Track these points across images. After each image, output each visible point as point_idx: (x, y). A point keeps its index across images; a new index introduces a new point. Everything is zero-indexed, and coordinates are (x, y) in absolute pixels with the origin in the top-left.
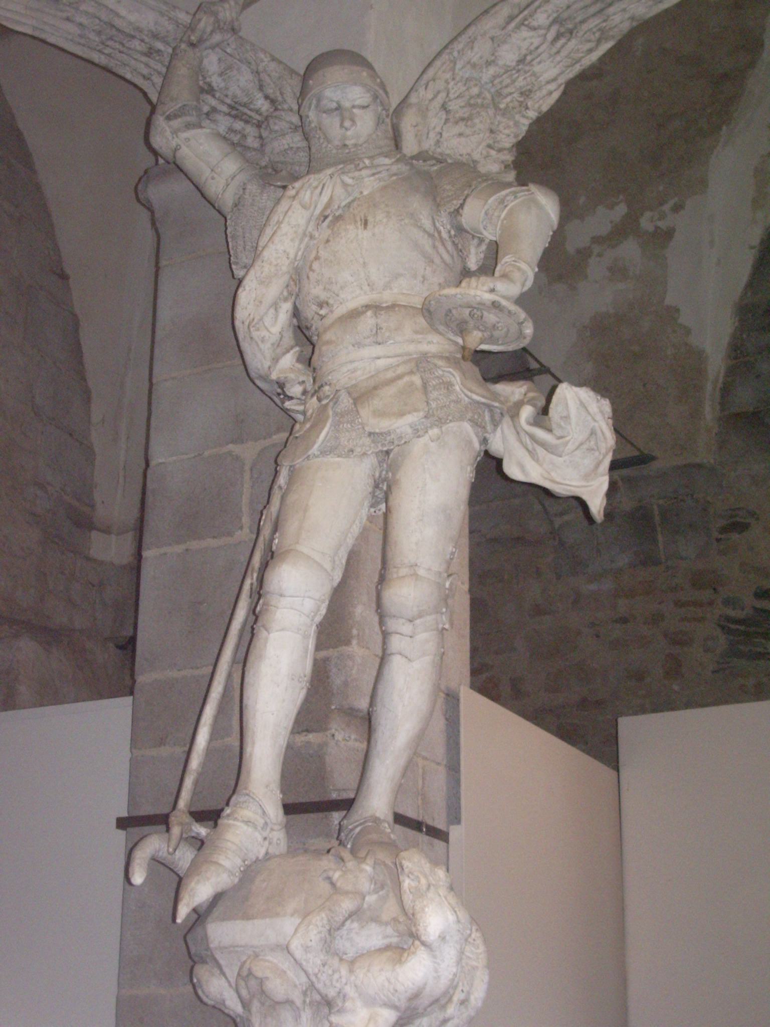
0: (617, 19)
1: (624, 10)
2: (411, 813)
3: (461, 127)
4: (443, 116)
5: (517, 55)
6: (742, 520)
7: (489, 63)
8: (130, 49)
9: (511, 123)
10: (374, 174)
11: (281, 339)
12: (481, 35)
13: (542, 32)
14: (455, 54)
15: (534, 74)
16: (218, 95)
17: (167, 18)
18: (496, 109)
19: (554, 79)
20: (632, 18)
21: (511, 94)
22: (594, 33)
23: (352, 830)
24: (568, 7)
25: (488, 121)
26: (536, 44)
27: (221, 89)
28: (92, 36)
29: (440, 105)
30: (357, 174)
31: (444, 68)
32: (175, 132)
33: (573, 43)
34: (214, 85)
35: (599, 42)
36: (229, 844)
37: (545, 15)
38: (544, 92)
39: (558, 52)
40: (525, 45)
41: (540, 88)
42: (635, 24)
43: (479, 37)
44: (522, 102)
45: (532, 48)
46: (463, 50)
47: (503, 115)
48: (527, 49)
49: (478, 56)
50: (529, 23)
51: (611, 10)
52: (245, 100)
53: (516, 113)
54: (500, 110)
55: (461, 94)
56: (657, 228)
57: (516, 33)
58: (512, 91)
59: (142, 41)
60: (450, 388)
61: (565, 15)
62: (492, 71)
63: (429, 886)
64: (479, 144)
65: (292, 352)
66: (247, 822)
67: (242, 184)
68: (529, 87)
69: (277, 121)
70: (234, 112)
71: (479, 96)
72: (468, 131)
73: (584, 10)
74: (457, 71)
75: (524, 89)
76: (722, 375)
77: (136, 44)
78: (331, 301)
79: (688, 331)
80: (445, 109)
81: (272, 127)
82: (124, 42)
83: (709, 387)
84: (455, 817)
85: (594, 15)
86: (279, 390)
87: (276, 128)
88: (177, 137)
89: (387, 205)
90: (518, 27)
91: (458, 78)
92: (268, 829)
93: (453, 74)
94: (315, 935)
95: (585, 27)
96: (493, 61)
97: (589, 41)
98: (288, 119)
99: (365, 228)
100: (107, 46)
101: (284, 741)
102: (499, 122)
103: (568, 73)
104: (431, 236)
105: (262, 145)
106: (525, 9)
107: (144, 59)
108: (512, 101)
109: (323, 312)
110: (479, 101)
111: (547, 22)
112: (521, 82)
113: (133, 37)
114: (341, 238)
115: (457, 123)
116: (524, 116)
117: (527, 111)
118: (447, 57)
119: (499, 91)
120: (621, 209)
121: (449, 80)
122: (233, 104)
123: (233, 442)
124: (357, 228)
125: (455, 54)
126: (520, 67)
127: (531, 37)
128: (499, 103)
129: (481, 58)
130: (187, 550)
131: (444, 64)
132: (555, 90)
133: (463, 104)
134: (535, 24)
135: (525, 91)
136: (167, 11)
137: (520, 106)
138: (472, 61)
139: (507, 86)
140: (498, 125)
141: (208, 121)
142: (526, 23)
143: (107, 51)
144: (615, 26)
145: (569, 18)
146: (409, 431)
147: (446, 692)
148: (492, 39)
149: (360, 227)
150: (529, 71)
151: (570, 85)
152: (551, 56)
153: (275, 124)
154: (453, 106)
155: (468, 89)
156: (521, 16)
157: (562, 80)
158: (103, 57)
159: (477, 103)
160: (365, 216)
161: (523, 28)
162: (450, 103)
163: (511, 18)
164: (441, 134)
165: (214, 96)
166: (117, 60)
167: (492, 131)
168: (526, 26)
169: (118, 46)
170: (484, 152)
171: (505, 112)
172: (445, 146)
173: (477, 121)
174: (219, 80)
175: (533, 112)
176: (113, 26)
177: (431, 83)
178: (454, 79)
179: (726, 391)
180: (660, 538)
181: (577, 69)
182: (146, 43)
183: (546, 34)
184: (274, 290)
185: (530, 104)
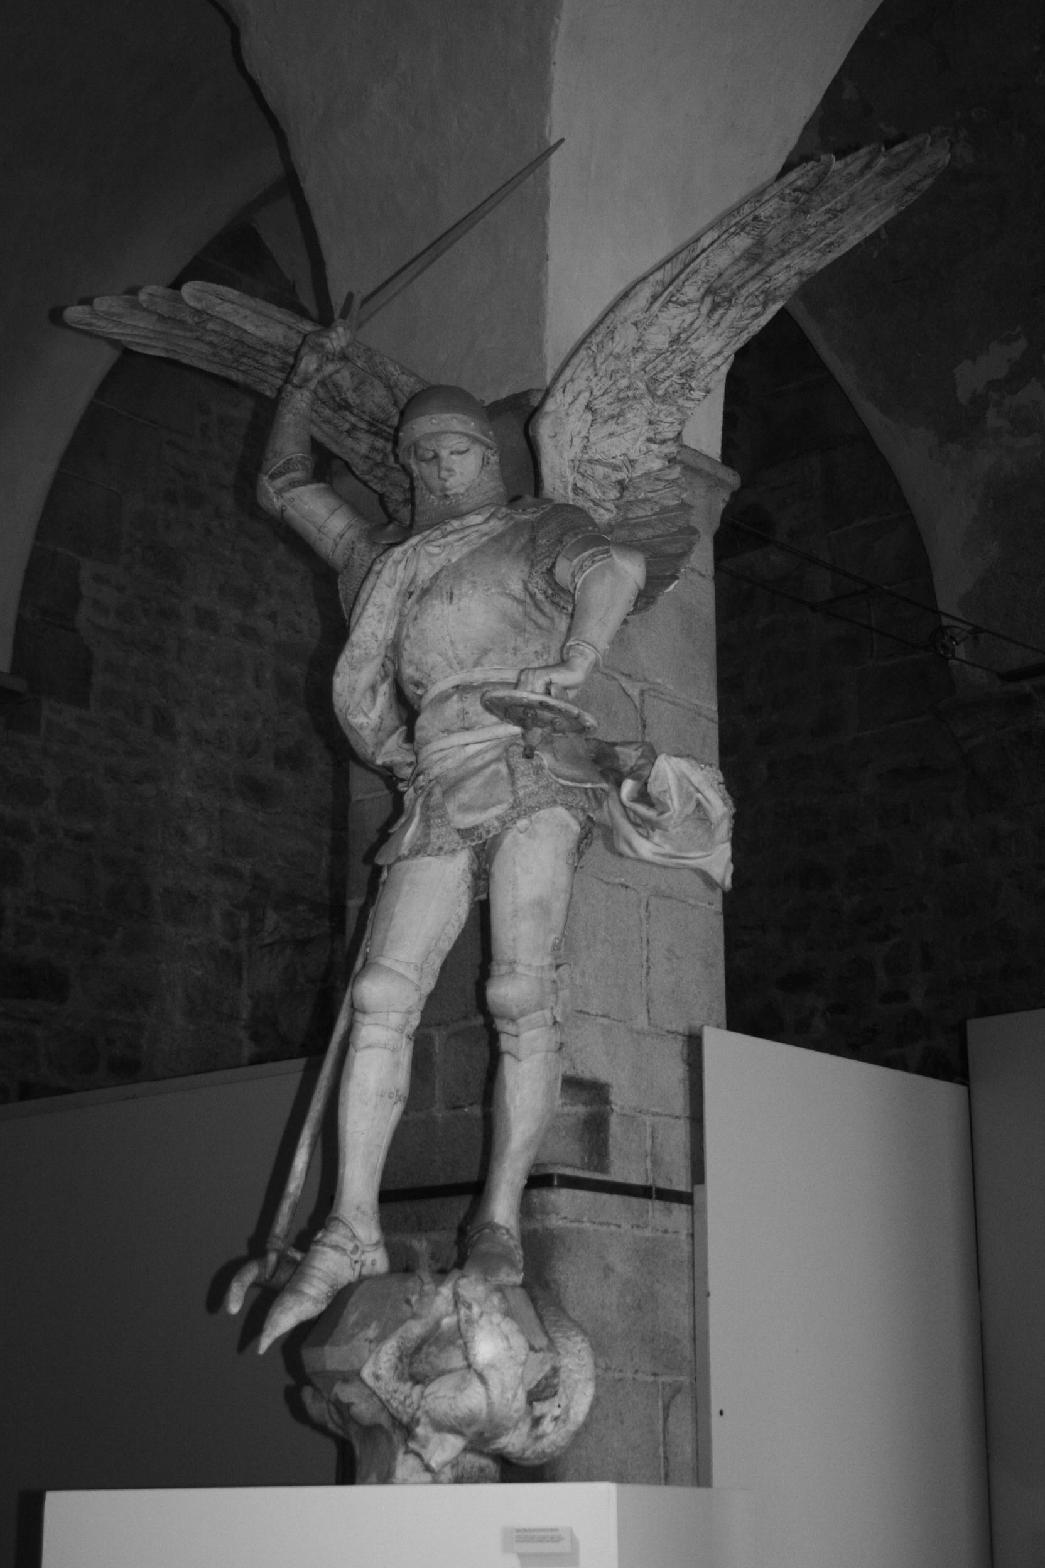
0: (782, 277)
3: (611, 426)
4: (589, 417)
5: (668, 336)
7: (635, 351)
8: (263, 365)
9: (674, 409)
10: (462, 539)
11: (381, 723)
12: (622, 323)
13: (696, 306)
14: (594, 348)
15: (693, 352)
16: (355, 411)
17: (295, 331)
18: (653, 397)
19: (720, 353)
20: (800, 273)
21: (668, 378)
22: (757, 297)
23: (473, 1236)
24: (720, 275)
25: (645, 413)
27: (358, 405)
28: (225, 354)
29: (583, 407)
30: (442, 541)
31: (583, 365)
32: (280, 492)
33: (733, 313)
34: (350, 401)
35: (765, 305)
38: (709, 368)
39: (718, 324)
40: (675, 324)
41: (703, 365)
42: (805, 279)
43: (619, 326)
44: (684, 384)
45: (685, 325)
46: (602, 342)
47: (663, 402)
48: (679, 328)
49: (621, 345)
50: (678, 299)
51: (772, 270)
52: (382, 416)
53: (679, 397)
55: (607, 389)
57: (663, 312)
58: (668, 375)
60: (540, 772)
62: (641, 357)
63: (481, 1315)
64: (636, 440)
65: (398, 732)
66: (336, 1247)
68: (689, 367)
70: (373, 430)
71: (628, 388)
72: (620, 429)
73: (740, 274)
74: (598, 365)
75: (683, 371)
77: (269, 360)
78: (424, 682)
84: (698, 1173)
85: (753, 278)
88: (282, 497)
90: (664, 306)
91: (601, 374)
92: (359, 1252)
93: (595, 370)
94: (385, 1363)
95: (744, 292)
96: (641, 348)
97: (754, 306)
99: (451, 603)
100: (241, 363)
101: (378, 1159)
102: (658, 410)
103: (735, 344)
104: (521, 602)
106: (670, 284)
108: (671, 385)
111: (699, 295)
112: (678, 363)
113: (266, 353)
114: (428, 615)
115: (606, 422)
116: (688, 399)
117: (692, 392)
118: (585, 353)
119: (654, 377)
121: (592, 377)
122: (371, 420)
124: (443, 603)
125: (594, 348)
126: (674, 347)
127: (682, 314)
128: (656, 390)
129: (625, 347)
132: (722, 364)
133: (611, 400)
134: (684, 299)
135: (686, 372)
136: (294, 323)
137: (683, 388)
138: (615, 352)
139: (662, 371)
140: (658, 415)
141: (350, 440)
142: (674, 299)
144: (781, 286)
145: (725, 285)
146: (496, 824)
147: (687, 1033)
148: (635, 324)
149: (445, 601)
150: (686, 350)
151: (740, 354)
152: (709, 329)
154: (599, 404)
156: (666, 293)
157: (729, 352)
159: (628, 396)
160: (451, 589)
162: (595, 402)
163: (655, 298)
164: (587, 438)
165: (352, 412)
166: (255, 377)
167: (651, 423)
168: (674, 302)
170: (644, 448)
171: (664, 399)
172: (594, 450)
173: (629, 416)
174: (354, 396)
176: (243, 343)
177: (568, 385)
178: (596, 375)
181: (745, 337)
183: (699, 308)
184: (368, 674)
185: (693, 384)
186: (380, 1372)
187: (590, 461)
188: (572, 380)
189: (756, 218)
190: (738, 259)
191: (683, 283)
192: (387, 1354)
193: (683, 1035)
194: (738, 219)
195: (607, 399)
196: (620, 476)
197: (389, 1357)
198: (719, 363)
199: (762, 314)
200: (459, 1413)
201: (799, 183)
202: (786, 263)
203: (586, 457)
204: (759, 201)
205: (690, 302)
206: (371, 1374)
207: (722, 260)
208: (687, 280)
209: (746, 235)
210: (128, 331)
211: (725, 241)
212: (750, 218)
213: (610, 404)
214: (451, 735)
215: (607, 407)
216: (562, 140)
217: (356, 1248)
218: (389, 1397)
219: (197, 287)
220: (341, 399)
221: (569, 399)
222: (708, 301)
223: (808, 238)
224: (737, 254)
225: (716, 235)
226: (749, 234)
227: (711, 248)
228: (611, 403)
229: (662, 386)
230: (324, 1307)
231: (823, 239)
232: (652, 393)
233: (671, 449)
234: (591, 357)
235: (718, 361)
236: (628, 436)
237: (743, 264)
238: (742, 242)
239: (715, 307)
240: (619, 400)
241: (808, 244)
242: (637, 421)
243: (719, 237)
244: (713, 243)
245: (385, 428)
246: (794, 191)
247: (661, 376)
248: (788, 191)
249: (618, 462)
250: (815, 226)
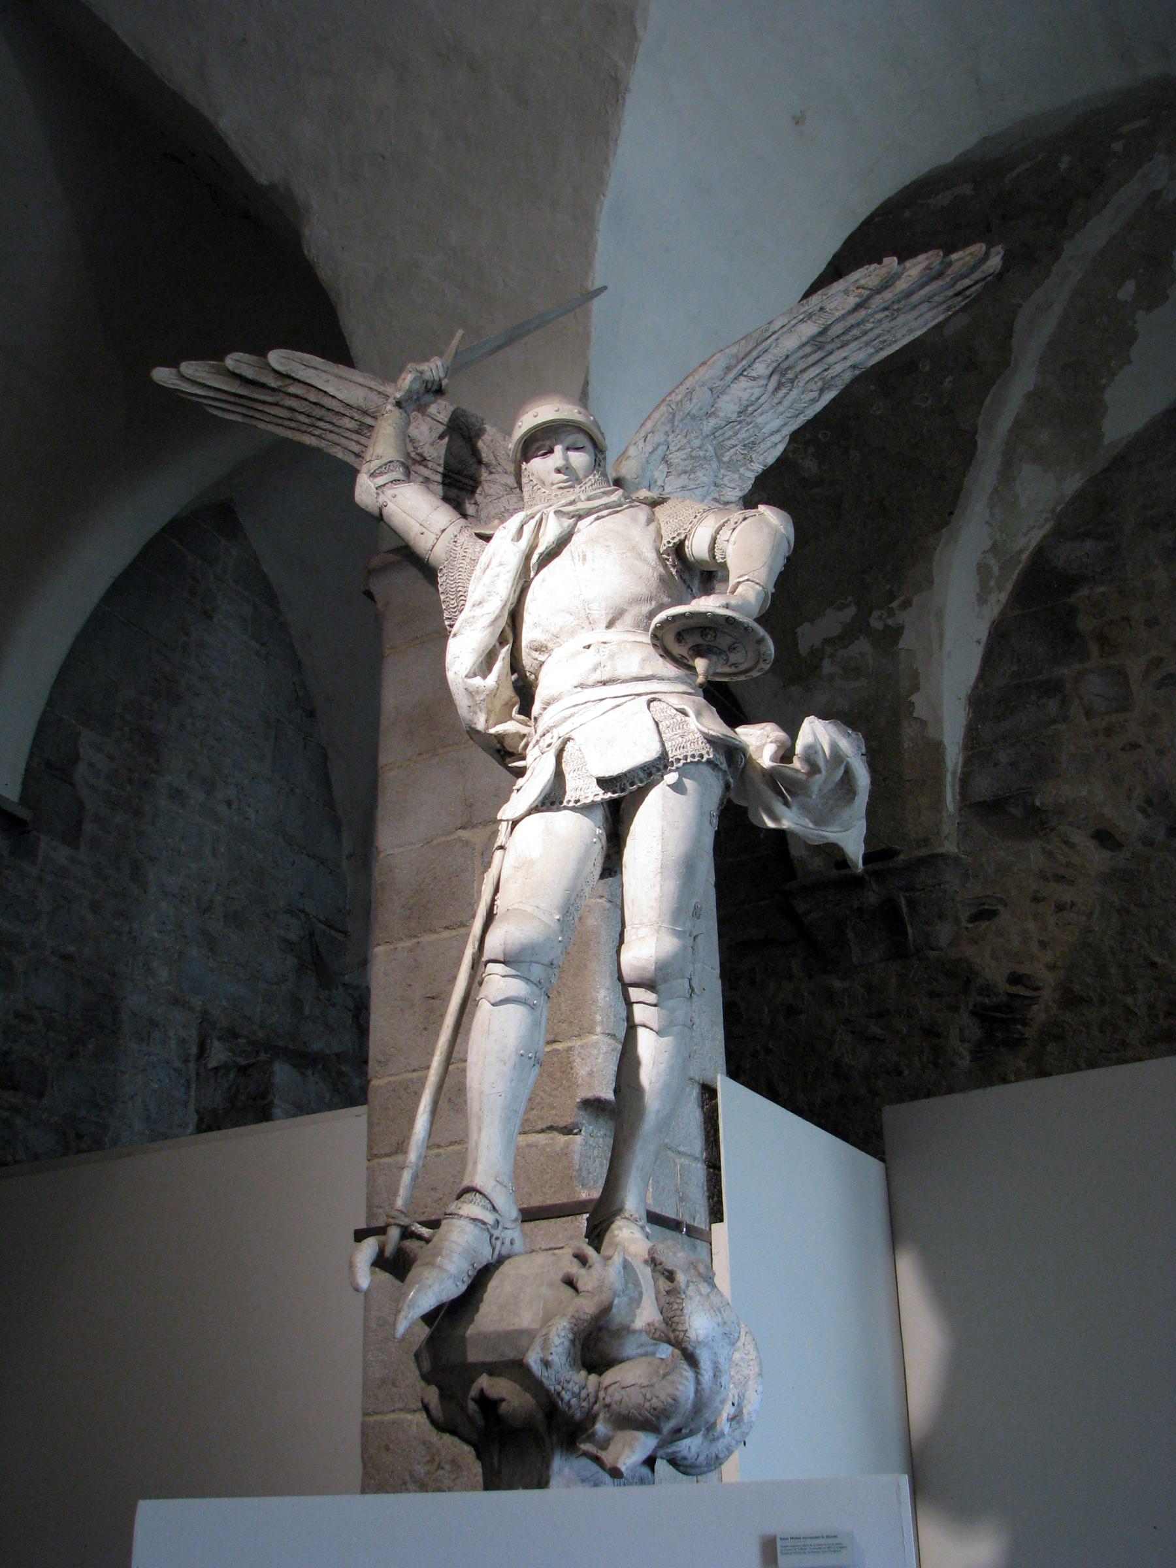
0: (838, 368)
1: (845, 358)
2: (669, 1212)
3: (683, 480)
5: (737, 406)
6: (991, 908)
7: (708, 415)
9: (736, 476)
13: (763, 382)
15: (756, 426)
16: (430, 464)
19: (778, 431)
20: (854, 367)
21: (734, 446)
24: (787, 357)
26: (756, 395)
34: (426, 455)
35: (822, 391)
36: (454, 1246)
37: (764, 366)
38: (768, 444)
39: (780, 403)
40: (745, 395)
42: (857, 372)
43: (697, 388)
45: (753, 399)
46: (681, 401)
48: (748, 400)
53: (741, 466)
54: (724, 463)
56: (886, 626)
59: (352, 418)
60: (685, 727)
61: (785, 365)
62: (713, 422)
67: (452, 537)
68: (752, 439)
69: (492, 485)
74: (676, 423)
76: (960, 765)
79: (923, 723)
80: (667, 462)
81: (486, 491)
82: (335, 421)
83: (949, 778)
84: (716, 1214)
85: (813, 365)
86: (498, 746)
87: (491, 491)
89: (606, 540)
91: (677, 432)
93: (673, 426)
96: (713, 413)
97: (812, 391)
98: (503, 481)
99: (583, 564)
105: (477, 511)
107: (355, 437)
109: (542, 658)
110: (702, 453)
111: (768, 372)
116: (748, 469)
120: (852, 610)
123: (463, 828)
125: (674, 406)
126: (742, 418)
127: (753, 387)
128: (722, 455)
129: (701, 409)
130: (418, 943)
133: (684, 457)
134: (754, 374)
138: (691, 413)
139: (729, 439)
142: (745, 373)
143: (317, 432)
145: (790, 368)
151: (795, 436)
153: (491, 488)
154: (676, 458)
155: (689, 442)
156: (739, 367)
158: (313, 438)
161: (742, 378)
162: (671, 456)
163: (728, 369)
165: (426, 466)
167: (716, 485)
168: (746, 376)
169: (328, 426)
171: (731, 466)
173: (699, 474)
174: (431, 450)
175: (758, 465)
177: (649, 435)
178: (673, 431)
179: (965, 781)
180: (910, 931)
182: (356, 420)
183: (766, 385)
185: (753, 456)
186: (550, 1358)
188: (653, 432)
189: (822, 309)
190: (804, 345)
191: (755, 360)
192: (558, 1335)
194: (807, 308)
195: (682, 454)
197: (562, 1340)
198: (777, 441)
199: (818, 401)
200: (655, 1402)
201: (862, 282)
202: (844, 354)
204: (825, 295)
205: (759, 377)
206: (539, 1362)
207: (790, 343)
208: (758, 358)
209: (812, 324)
211: (793, 326)
212: (819, 306)
214: (585, 690)
215: (682, 463)
216: (605, 288)
218: (559, 1388)
219: (283, 355)
220: (417, 454)
222: (775, 378)
223: (865, 333)
224: (804, 339)
225: (786, 321)
226: (815, 322)
227: (780, 332)
228: (685, 460)
229: (728, 453)
230: (463, 1288)
231: (879, 336)
232: (719, 457)
234: (671, 413)
235: (776, 438)
237: (808, 349)
238: (809, 329)
240: (692, 457)
241: (865, 338)
242: (705, 479)
243: (789, 322)
244: (783, 326)
245: (460, 478)
246: (857, 288)
247: (729, 443)
250: (873, 322)
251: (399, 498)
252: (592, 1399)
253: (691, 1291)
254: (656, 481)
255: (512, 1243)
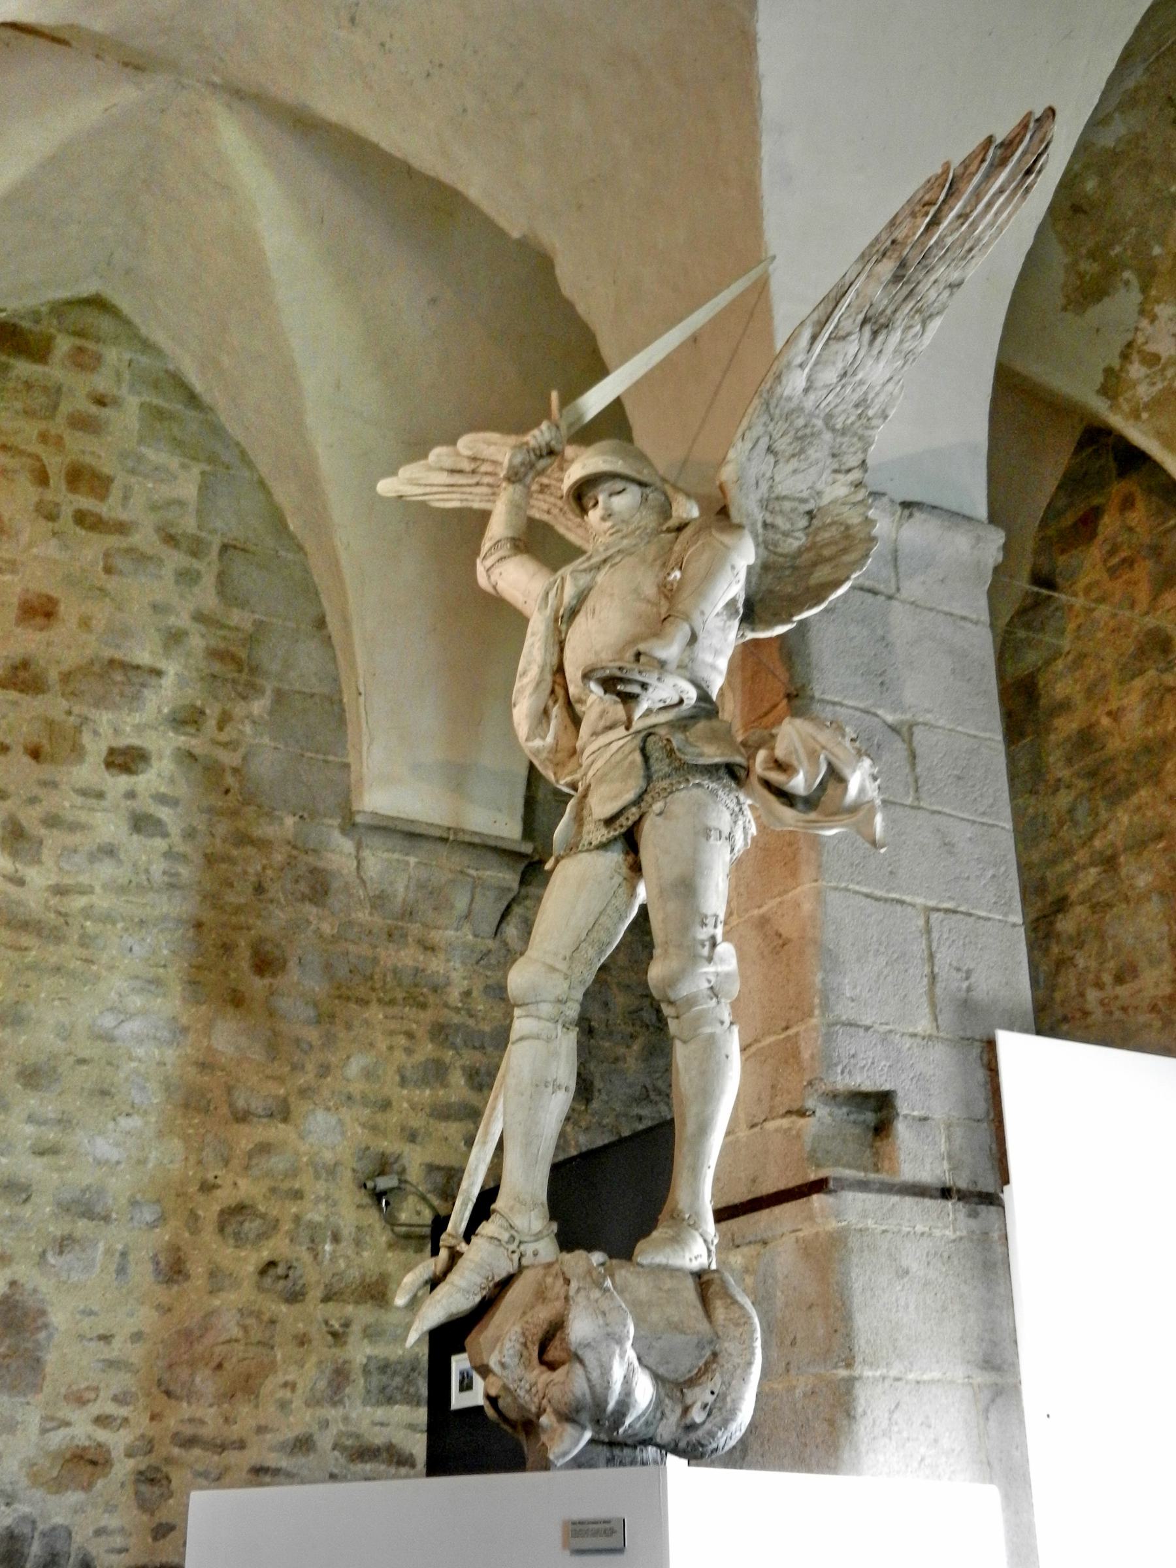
3: (794, 463)
9: (855, 440)
14: (765, 395)
29: (764, 451)
46: (771, 388)
63: (578, 1290)
71: (806, 426)
72: (803, 465)
91: (776, 417)
115: (788, 461)
131: (755, 409)
139: (836, 406)
154: (781, 445)
161: (831, 342)
167: (834, 456)
170: (830, 480)
178: (772, 420)
187: (777, 498)
188: (749, 428)
189: (893, 242)
193: (981, 1041)
196: (808, 507)
203: (773, 495)
210: (428, 490)
212: (889, 242)
213: (791, 444)
217: (513, 1238)
221: (749, 445)
222: (867, 330)
233: (855, 475)
236: (813, 470)
238: (887, 268)
239: (875, 334)
242: (819, 455)
248: (917, 208)
249: (805, 495)
251: (504, 574)
252: (541, 1395)
253: (581, 1299)
254: (763, 475)
255: (536, 1254)
